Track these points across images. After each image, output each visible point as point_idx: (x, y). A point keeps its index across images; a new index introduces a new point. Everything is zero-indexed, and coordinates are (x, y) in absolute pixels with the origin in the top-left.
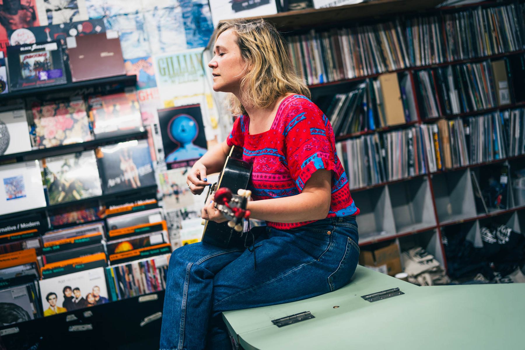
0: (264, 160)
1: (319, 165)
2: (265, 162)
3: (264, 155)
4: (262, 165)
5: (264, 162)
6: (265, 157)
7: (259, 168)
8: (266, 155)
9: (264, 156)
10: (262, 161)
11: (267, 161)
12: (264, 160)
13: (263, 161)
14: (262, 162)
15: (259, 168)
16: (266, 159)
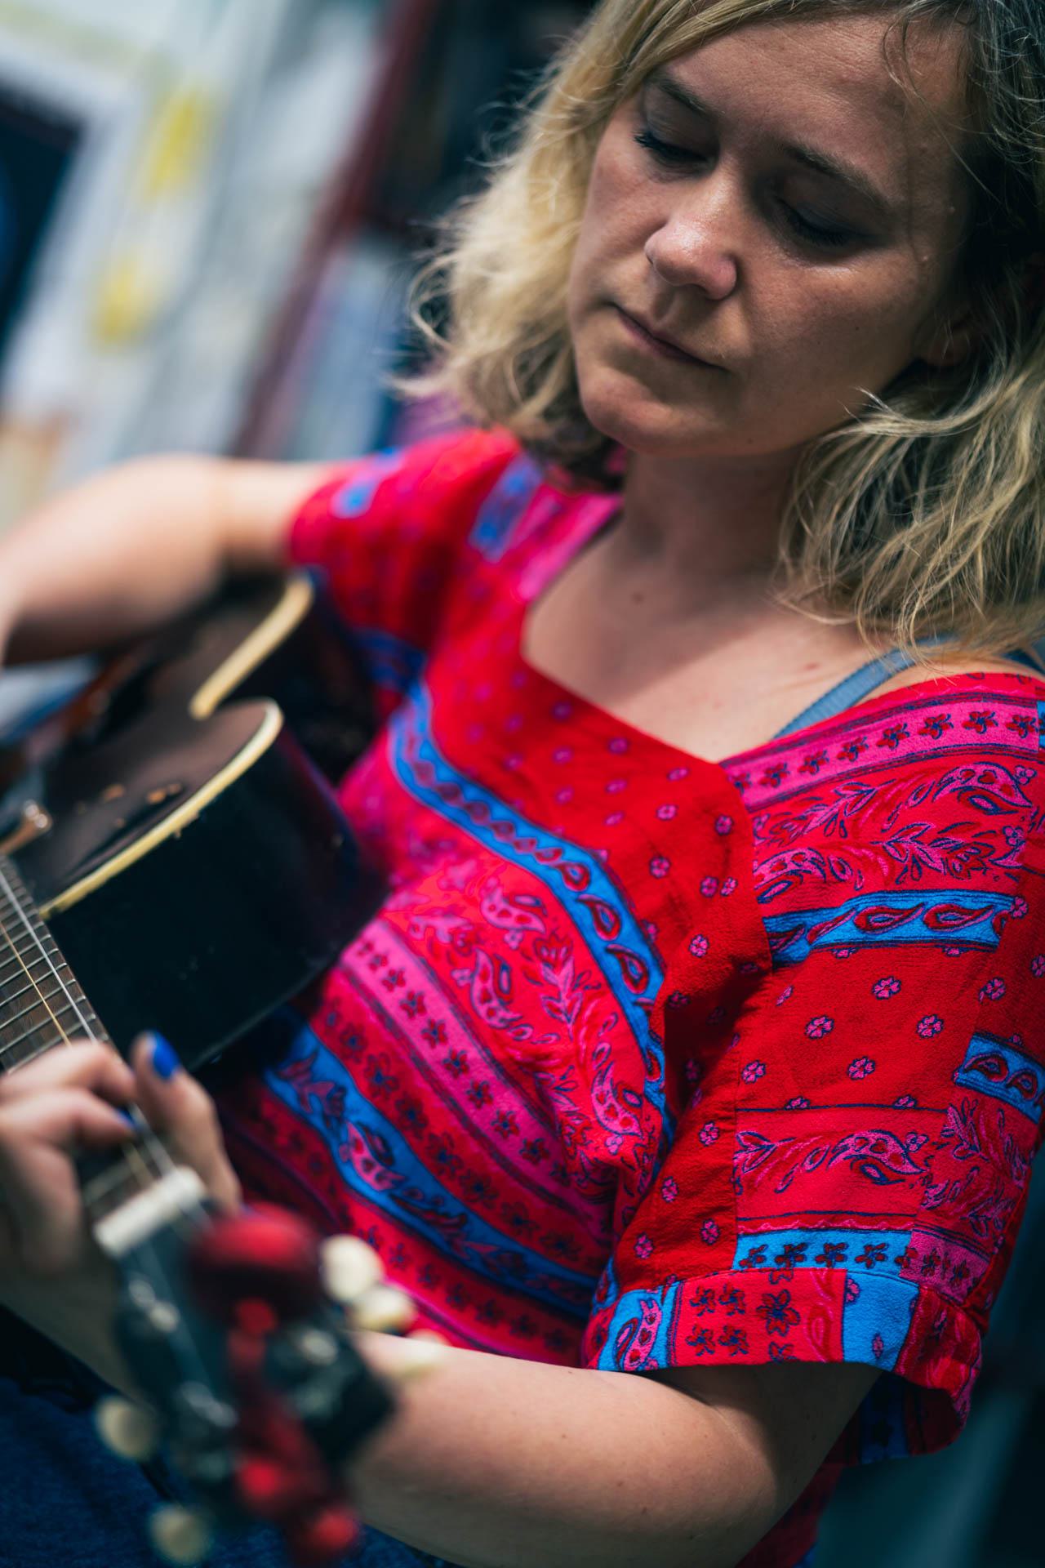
0: (520, 919)
1: (877, 1336)
2: (513, 941)
3: (545, 886)
4: (474, 939)
5: (506, 930)
6: (539, 910)
7: (444, 937)
8: (560, 903)
9: (545, 903)
10: (504, 914)
11: (536, 948)
12: (520, 919)
13: (508, 923)
14: (492, 917)
15: (444, 937)
16: (537, 924)
